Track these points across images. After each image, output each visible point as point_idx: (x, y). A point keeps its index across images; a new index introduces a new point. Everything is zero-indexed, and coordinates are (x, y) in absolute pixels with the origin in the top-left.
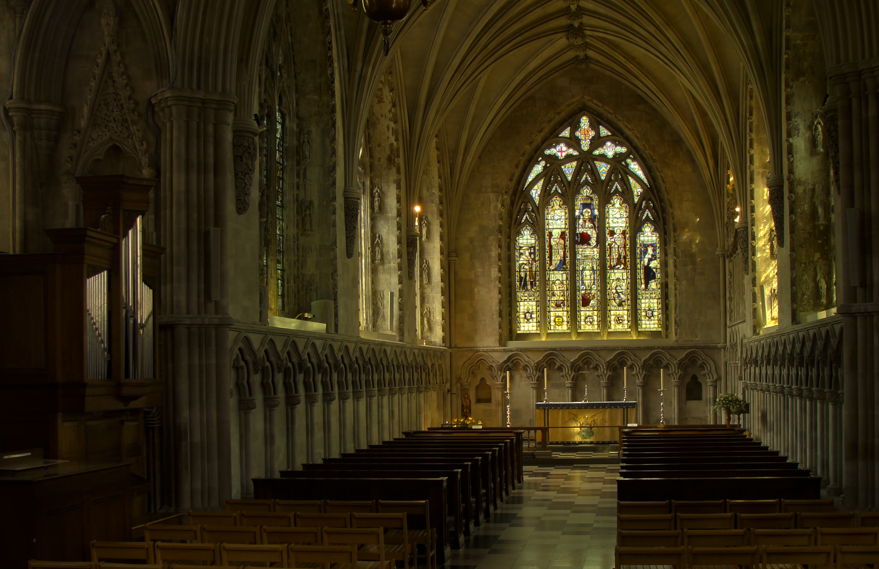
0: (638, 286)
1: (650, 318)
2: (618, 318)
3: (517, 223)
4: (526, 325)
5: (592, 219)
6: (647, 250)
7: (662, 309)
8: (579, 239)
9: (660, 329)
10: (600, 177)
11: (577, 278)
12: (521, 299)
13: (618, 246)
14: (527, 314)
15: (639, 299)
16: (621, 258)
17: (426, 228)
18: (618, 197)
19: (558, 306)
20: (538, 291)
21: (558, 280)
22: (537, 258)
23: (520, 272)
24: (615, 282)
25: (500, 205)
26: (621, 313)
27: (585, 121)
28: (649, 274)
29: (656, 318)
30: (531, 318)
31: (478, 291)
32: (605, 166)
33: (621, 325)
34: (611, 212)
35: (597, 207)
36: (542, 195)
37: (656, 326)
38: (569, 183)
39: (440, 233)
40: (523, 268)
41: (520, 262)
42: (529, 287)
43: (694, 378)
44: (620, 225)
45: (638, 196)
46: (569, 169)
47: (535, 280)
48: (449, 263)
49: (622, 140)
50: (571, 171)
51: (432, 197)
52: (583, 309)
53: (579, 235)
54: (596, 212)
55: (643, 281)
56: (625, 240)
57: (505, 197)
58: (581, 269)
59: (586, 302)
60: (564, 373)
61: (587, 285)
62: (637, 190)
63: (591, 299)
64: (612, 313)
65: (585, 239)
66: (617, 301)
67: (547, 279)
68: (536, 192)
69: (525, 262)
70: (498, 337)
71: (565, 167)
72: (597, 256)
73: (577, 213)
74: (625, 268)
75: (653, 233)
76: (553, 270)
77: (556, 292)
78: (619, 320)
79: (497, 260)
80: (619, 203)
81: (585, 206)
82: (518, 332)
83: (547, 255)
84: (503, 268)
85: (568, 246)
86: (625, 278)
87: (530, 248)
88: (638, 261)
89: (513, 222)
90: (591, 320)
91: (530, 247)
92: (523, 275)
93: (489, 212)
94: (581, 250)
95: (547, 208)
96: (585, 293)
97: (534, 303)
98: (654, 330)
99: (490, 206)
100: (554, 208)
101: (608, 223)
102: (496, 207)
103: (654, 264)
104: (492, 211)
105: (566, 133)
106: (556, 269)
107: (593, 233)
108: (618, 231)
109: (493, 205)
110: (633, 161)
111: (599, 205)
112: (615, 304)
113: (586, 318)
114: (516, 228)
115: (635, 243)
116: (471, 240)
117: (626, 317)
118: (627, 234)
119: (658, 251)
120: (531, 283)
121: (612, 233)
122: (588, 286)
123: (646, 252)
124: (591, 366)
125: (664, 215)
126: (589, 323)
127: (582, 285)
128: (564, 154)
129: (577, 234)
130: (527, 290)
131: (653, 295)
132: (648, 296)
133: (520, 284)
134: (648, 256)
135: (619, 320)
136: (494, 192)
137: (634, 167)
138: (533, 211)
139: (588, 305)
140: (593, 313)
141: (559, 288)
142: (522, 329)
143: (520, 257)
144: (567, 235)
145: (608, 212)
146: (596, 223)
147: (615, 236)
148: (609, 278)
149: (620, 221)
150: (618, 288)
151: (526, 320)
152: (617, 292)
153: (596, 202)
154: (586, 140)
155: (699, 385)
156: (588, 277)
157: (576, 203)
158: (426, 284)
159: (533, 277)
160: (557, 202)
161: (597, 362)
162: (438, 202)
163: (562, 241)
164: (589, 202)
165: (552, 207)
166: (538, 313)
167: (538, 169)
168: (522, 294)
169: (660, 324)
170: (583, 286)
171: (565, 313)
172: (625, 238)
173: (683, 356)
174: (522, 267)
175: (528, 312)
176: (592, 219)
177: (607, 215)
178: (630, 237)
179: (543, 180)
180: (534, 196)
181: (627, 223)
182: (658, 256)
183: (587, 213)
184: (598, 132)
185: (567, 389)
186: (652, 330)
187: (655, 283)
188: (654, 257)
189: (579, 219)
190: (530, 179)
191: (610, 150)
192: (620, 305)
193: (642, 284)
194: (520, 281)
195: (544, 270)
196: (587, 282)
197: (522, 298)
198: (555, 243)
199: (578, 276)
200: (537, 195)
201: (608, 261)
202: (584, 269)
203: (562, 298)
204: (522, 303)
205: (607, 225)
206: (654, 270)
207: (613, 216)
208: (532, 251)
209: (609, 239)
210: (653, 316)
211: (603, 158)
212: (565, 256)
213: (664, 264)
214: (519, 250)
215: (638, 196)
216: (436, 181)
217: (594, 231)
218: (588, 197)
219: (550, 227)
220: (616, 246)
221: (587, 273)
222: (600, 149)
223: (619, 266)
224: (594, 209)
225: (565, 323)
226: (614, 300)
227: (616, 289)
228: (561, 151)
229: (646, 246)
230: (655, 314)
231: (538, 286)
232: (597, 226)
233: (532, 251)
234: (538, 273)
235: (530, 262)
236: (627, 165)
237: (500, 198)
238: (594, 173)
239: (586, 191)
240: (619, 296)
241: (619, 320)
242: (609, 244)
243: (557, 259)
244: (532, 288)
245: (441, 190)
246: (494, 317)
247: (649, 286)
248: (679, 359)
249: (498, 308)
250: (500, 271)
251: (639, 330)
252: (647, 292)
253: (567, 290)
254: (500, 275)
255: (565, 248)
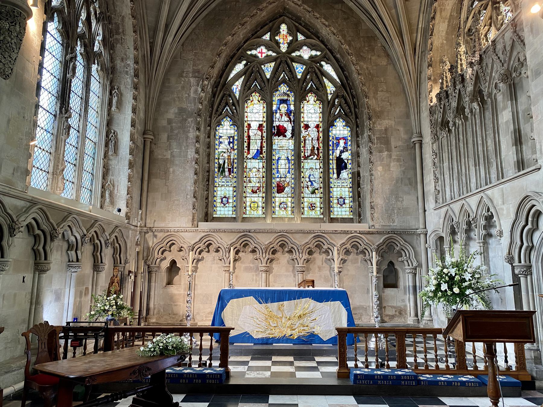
0: (331, 176)
1: (341, 205)
2: (311, 204)
3: (218, 113)
4: (222, 209)
5: (288, 114)
6: (339, 143)
7: (353, 197)
8: (276, 131)
9: (352, 217)
10: (296, 76)
11: (274, 167)
12: (219, 185)
13: (312, 138)
14: (224, 199)
15: (331, 187)
16: (314, 150)
17: (116, 98)
18: (313, 94)
19: (254, 192)
20: (235, 177)
21: (254, 168)
22: (235, 147)
23: (219, 159)
24: (308, 171)
25: (200, 90)
26: (314, 200)
27: (284, 28)
28: (341, 165)
29: (348, 206)
30: (228, 202)
31: (174, 171)
32: (301, 67)
33: (314, 211)
34: (305, 108)
35: (293, 103)
36: (242, 91)
37: (348, 213)
38: (268, 80)
39: (133, 104)
40: (222, 156)
41: (219, 150)
42: (227, 173)
43: (391, 264)
44: (314, 119)
45: (331, 94)
46: (268, 70)
47: (233, 168)
48: (144, 141)
49: (317, 42)
50: (271, 69)
51: (127, 68)
52: (277, 195)
53: (276, 128)
54: (292, 108)
55: (335, 171)
56: (319, 133)
57: (205, 82)
58: (277, 158)
59: (281, 189)
60: (258, 256)
61: (282, 173)
62: (330, 88)
63: (285, 186)
64: (306, 199)
65: (281, 132)
66: (310, 189)
67: (244, 167)
68: (237, 87)
69: (224, 151)
70: (191, 218)
71: (265, 66)
72: (292, 147)
73: (274, 108)
74: (318, 158)
75: (344, 127)
76: (250, 159)
77: (252, 178)
78: (313, 206)
79: (195, 141)
80: (313, 100)
81: (282, 101)
82: (214, 216)
83: (246, 144)
84: (201, 151)
85: (265, 137)
86: (318, 167)
87: (229, 137)
88: (331, 152)
89: (214, 111)
90: (285, 206)
91: (229, 137)
92: (221, 162)
93: (189, 95)
94: (276, 141)
95: (246, 102)
96: (280, 181)
97: (231, 189)
98: (346, 217)
99: (190, 89)
100: (253, 103)
101: (303, 117)
102: (196, 91)
103: (345, 156)
104: (192, 95)
105: (267, 37)
106: (253, 158)
107: (289, 127)
108: (312, 125)
109: (193, 89)
110: (327, 63)
111: (295, 101)
112: (308, 191)
113: (281, 204)
114: (217, 118)
115: (329, 136)
116: (170, 121)
117: (318, 204)
118: (320, 127)
119: (349, 143)
120: (229, 170)
121: (307, 127)
122: (284, 174)
123: (338, 144)
124: (286, 249)
125: (357, 110)
126: (283, 209)
127: (277, 173)
128: (264, 55)
129: (274, 127)
130: (225, 176)
131: (345, 184)
132: (338, 184)
133: (219, 171)
134: (341, 148)
135: (312, 207)
136: (195, 77)
137: (328, 68)
138: (233, 104)
139: (283, 191)
140: (287, 200)
141: (256, 175)
142: (218, 213)
143: (219, 146)
144: (264, 127)
145: (303, 107)
146: (292, 117)
147: (309, 129)
148: (303, 167)
149: (314, 116)
150: (312, 177)
151: (222, 205)
152: (310, 181)
153: (292, 99)
154: (284, 44)
155: (396, 272)
156: (283, 166)
157: (274, 98)
158: (112, 155)
159: (231, 165)
160: (256, 97)
161: (292, 245)
162: (133, 74)
163: (260, 133)
164: (286, 98)
165: (252, 101)
166: (234, 198)
167: (239, 67)
168: (220, 180)
169: (352, 211)
170: (278, 174)
171: (261, 199)
172: (318, 131)
173: (381, 241)
174: (221, 155)
175: (225, 197)
176: (288, 114)
177: (302, 110)
178: (323, 130)
179: (243, 77)
180: (235, 91)
181: (320, 117)
182: (349, 148)
183: (284, 108)
184: (295, 39)
185: (261, 272)
186: (343, 217)
187: (347, 173)
188: (345, 149)
189: (276, 113)
190: (232, 75)
191: (306, 53)
192: (313, 192)
193: (334, 173)
194: (219, 168)
195: (241, 158)
196: (281, 171)
197: (220, 183)
198: (253, 134)
199: (274, 165)
200: (237, 90)
201: (302, 152)
202: (279, 159)
203: (258, 185)
204: (219, 189)
205: (302, 120)
206: (346, 161)
207: (307, 111)
208: (231, 140)
209: (304, 133)
210: (344, 203)
211: (299, 60)
212: (262, 147)
213: (356, 155)
214: (219, 139)
215: (331, 94)
216: (131, 53)
217: (290, 124)
218: (285, 94)
219: (249, 119)
220: (310, 139)
221: (282, 162)
222: (297, 52)
223: (312, 157)
224: (290, 105)
225: (260, 208)
226: (308, 187)
227: (309, 178)
228: (262, 52)
229: (338, 139)
230: (347, 201)
231: (235, 173)
232: (292, 120)
233: (231, 140)
234: (236, 161)
235: (229, 150)
236: (322, 66)
237: (201, 83)
238: (292, 72)
239: (283, 88)
240: (312, 184)
241: (312, 207)
242: (303, 137)
243: (255, 147)
244: (230, 174)
245: (136, 62)
246: (188, 197)
247: (341, 175)
248: (377, 244)
249: (193, 188)
250: (197, 152)
251: (332, 216)
252: (338, 181)
253: (263, 177)
254: (197, 156)
255: (262, 139)
